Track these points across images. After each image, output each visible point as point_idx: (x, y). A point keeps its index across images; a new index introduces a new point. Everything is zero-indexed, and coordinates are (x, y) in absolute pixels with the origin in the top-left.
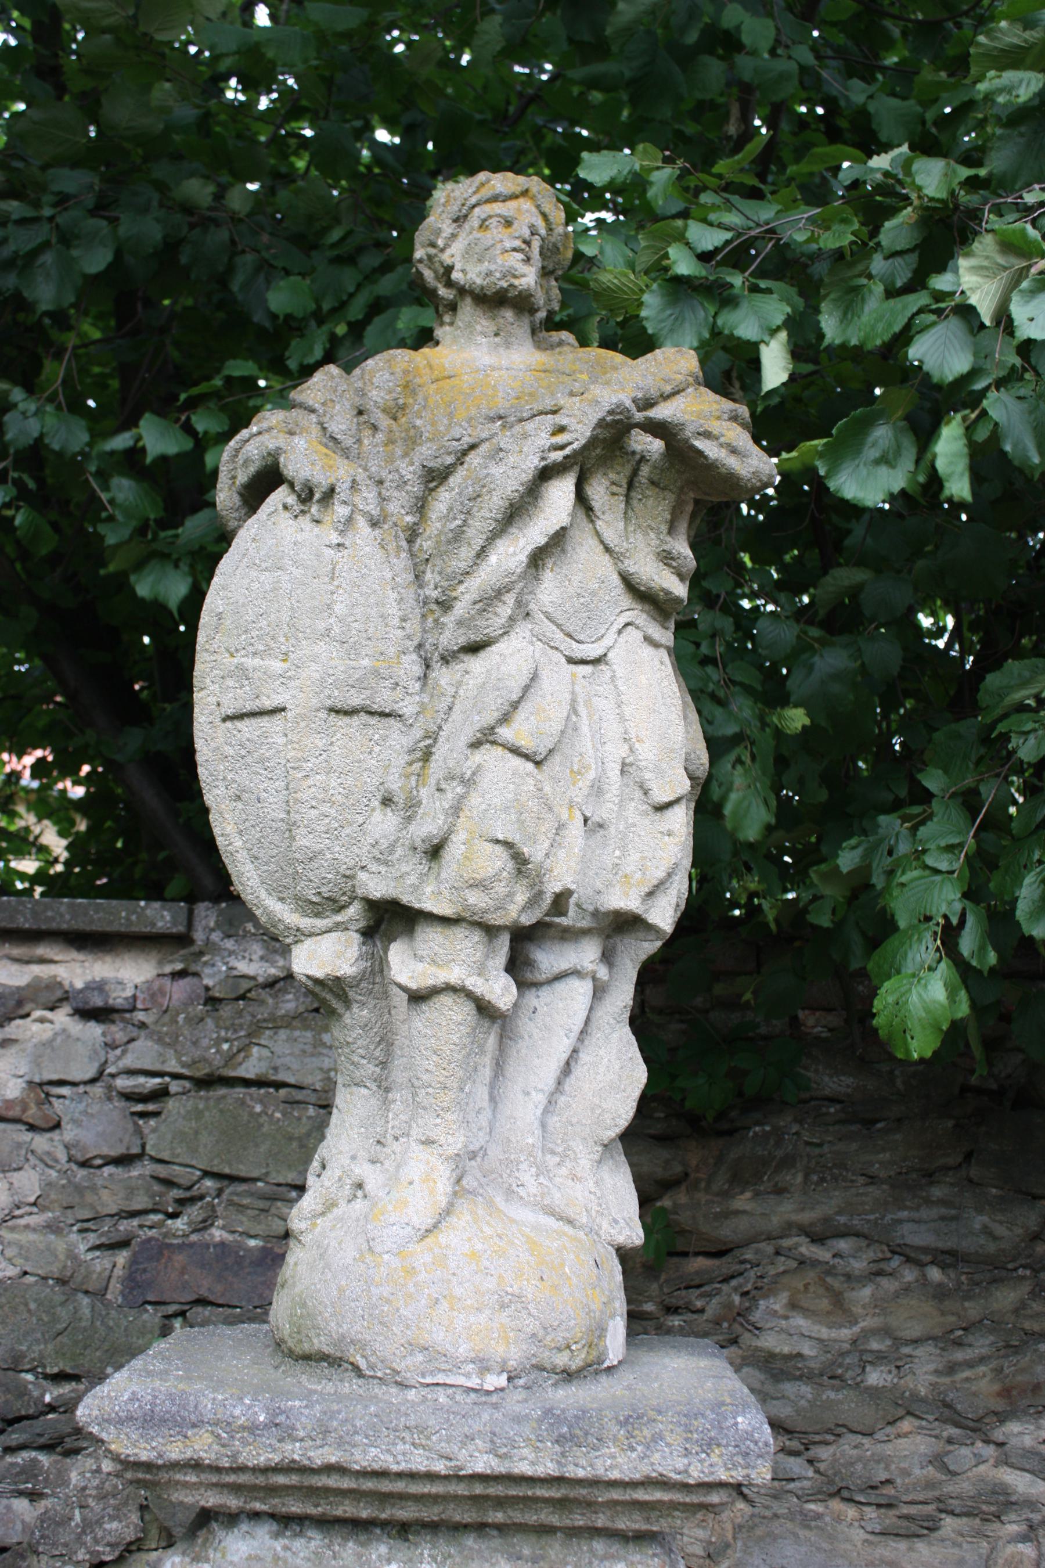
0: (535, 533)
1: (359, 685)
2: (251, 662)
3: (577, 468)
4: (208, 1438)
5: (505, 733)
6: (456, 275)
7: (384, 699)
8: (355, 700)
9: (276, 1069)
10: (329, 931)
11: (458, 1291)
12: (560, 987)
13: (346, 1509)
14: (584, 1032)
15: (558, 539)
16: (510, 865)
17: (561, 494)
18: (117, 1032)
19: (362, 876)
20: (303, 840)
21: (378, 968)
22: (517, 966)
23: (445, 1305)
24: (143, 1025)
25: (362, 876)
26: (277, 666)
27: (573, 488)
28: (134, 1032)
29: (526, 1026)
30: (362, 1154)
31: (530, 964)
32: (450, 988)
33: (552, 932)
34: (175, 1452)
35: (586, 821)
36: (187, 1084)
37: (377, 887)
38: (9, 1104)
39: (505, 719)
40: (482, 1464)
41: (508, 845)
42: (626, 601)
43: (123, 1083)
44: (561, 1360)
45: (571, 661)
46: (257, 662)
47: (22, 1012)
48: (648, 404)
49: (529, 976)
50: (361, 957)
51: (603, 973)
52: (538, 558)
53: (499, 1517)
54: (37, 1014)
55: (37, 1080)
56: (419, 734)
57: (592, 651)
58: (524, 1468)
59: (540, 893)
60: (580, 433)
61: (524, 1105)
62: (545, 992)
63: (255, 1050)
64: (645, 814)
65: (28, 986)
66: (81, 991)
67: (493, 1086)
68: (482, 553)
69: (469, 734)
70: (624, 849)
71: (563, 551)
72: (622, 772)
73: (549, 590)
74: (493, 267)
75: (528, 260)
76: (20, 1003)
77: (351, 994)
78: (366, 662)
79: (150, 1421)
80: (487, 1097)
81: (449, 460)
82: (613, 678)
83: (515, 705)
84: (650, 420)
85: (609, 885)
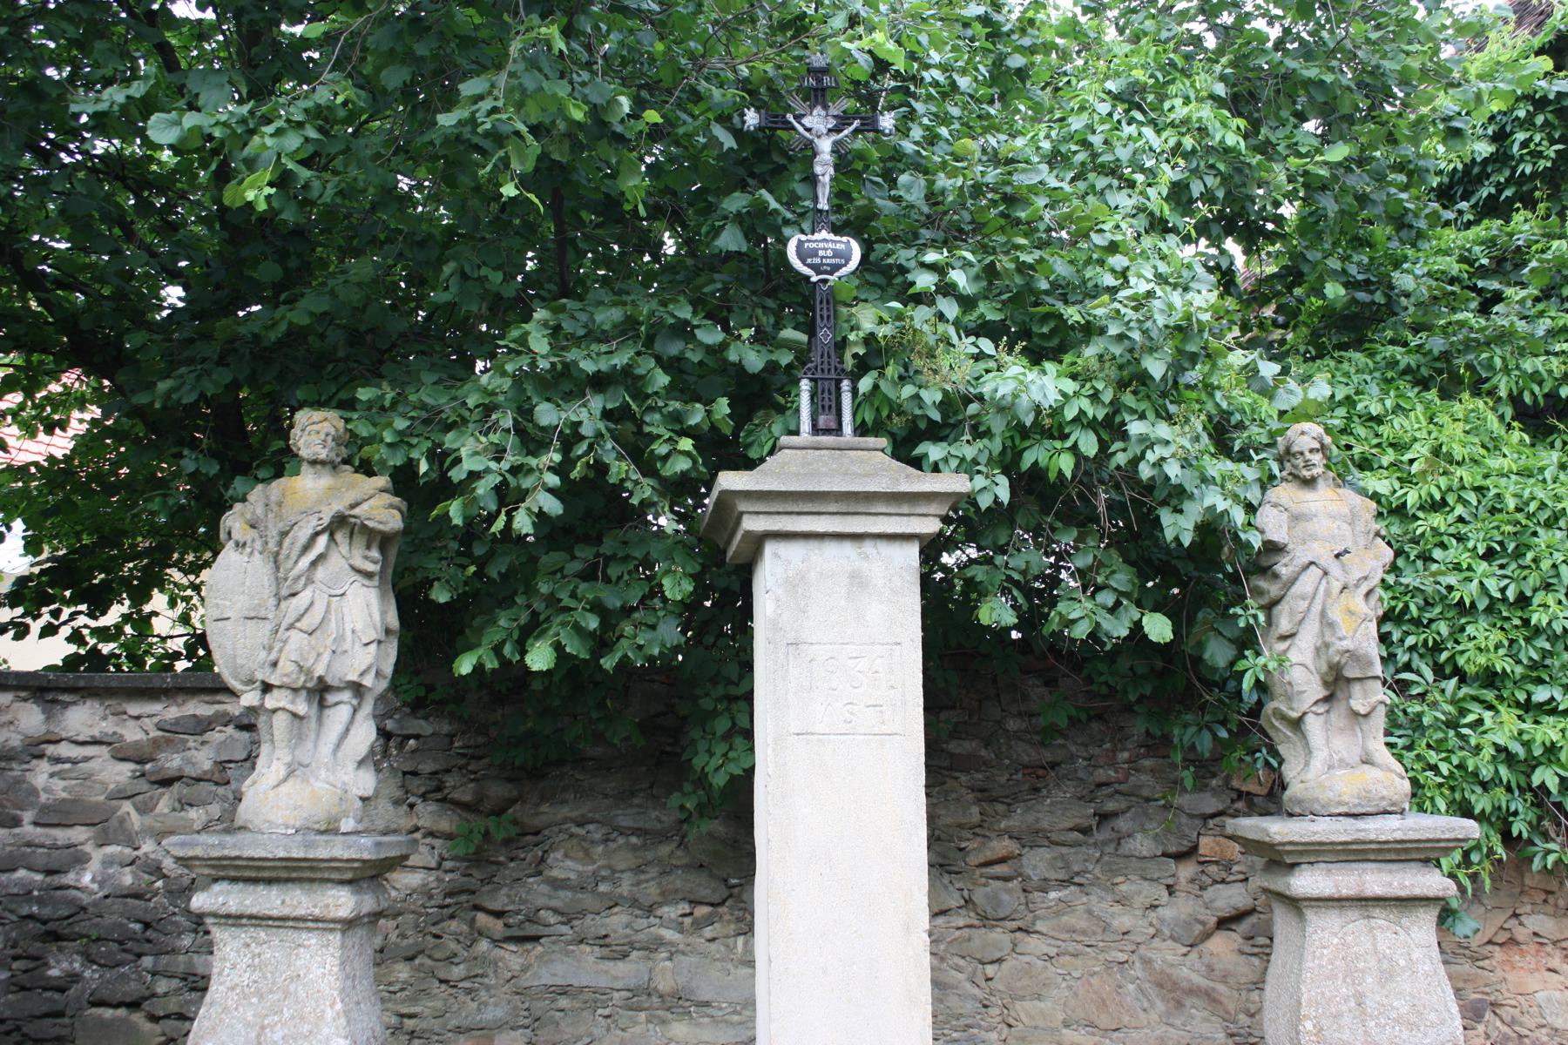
7: (262, 613)
13: (247, 874)
15: (321, 557)
20: (239, 661)
32: (283, 709)
34: (191, 854)
38: (205, 772)
39: (298, 620)
40: (282, 854)
52: (314, 564)
53: (294, 875)
58: (295, 855)
60: (326, 521)
73: (320, 573)
79: (183, 845)
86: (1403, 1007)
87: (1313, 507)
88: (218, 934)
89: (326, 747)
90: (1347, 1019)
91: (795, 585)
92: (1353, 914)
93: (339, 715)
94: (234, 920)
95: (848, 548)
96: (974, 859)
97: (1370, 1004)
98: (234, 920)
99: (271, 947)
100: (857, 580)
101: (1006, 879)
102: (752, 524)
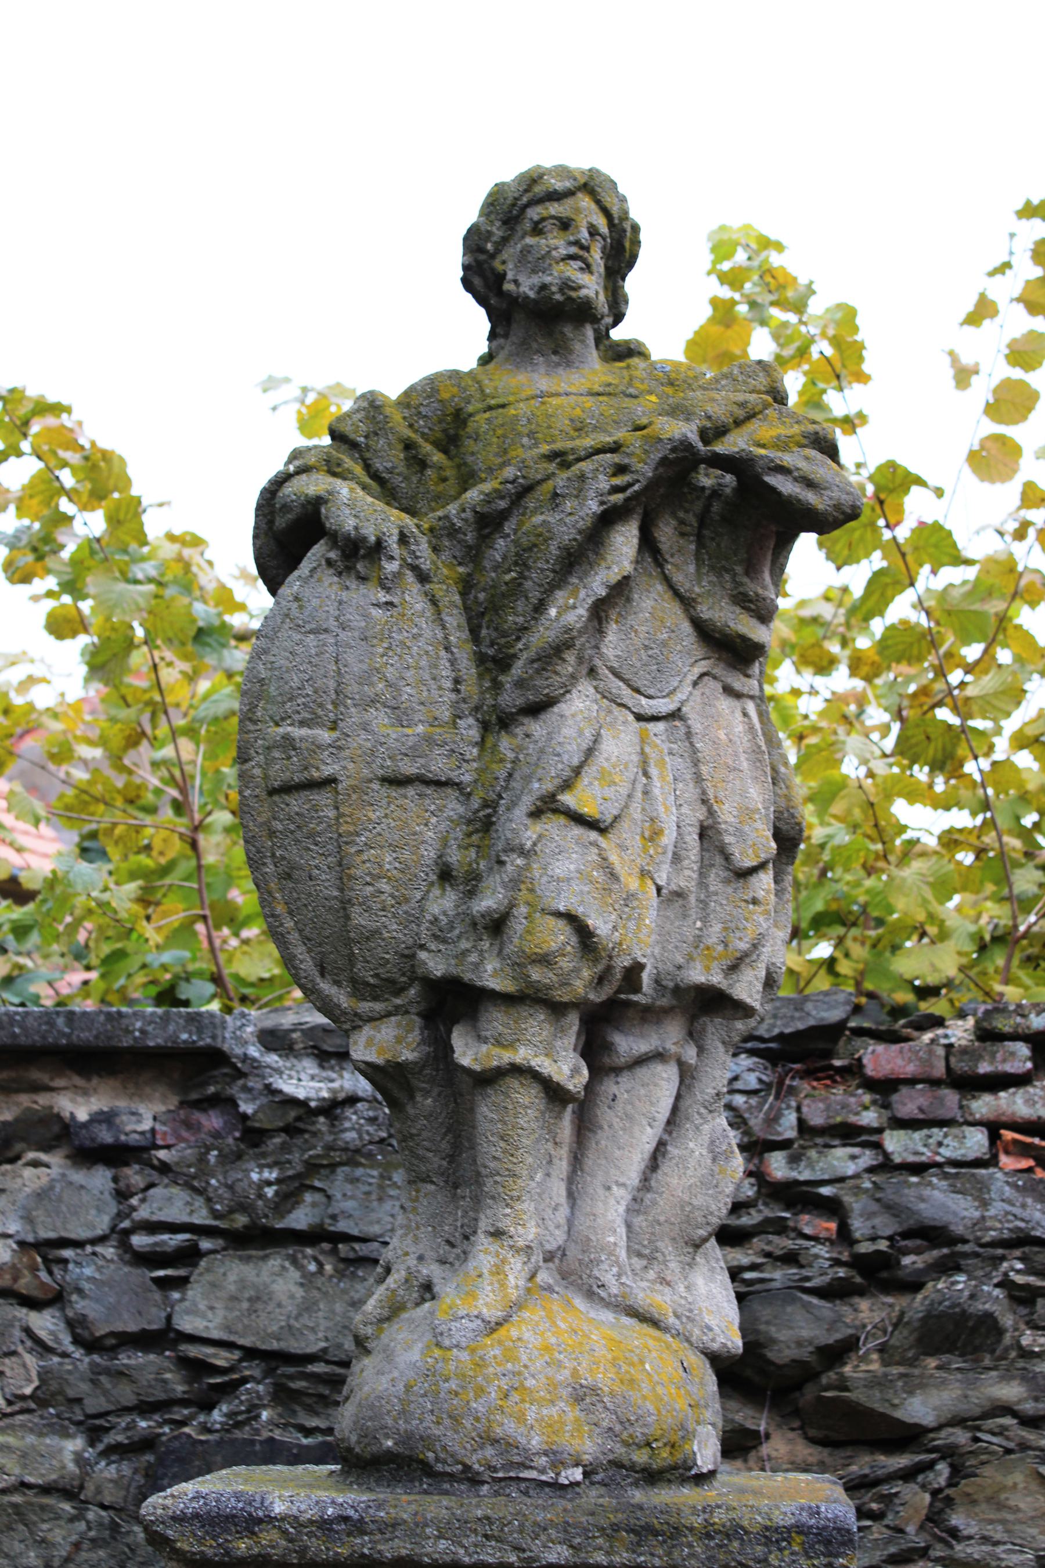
0: (598, 583)
1: (413, 753)
2: (298, 732)
3: (640, 510)
4: (275, 1535)
5: (567, 799)
6: (508, 287)
7: (439, 765)
8: (408, 768)
9: (334, 1217)
10: (389, 1014)
11: (530, 1383)
12: (642, 1072)
14: (672, 1122)
15: (621, 589)
16: (574, 940)
17: (624, 544)
18: (134, 1176)
19: (423, 955)
20: (359, 918)
21: (441, 1051)
22: (594, 1051)
23: (515, 1397)
24: (164, 1168)
25: (423, 955)
26: (325, 736)
27: (635, 532)
28: (155, 1176)
29: (606, 1116)
30: (430, 1254)
31: (608, 1047)
33: (631, 1013)
35: (659, 889)
36: (220, 1243)
37: (436, 965)
39: (567, 785)
41: (571, 918)
42: (699, 652)
43: (139, 1241)
44: (640, 1457)
45: (640, 718)
46: (304, 732)
47: (10, 1154)
48: (721, 432)
49: (607, 1060)
50: (423, 1042)
51: (690, 1054)
52: (600, 611)
54: (31, 1155)
55: (30, 1238)
56: (476, 803)
57: (663, 706)
59: (609, 969)
61: (610, 1211)
62: (625, 1079)
63: (308, 1197)
64: (727, 881)
65: (17, 1120)
66: (85, 1125)
67: (571, 1180)
68: (540, 608)
69: (527, 803)
70: (704, 919)
71: (629, 600)
72: (701, 836)
73: (613, 644)
74: (548, 279)
75: (588, 268)
76: (7, 1143)
77: (415, 1082)
78: (420, 729)
80: (563, 1192)
81: (503, 504)
82: (689, 735)
83: (577, 771)
84: (716, 455)
85: (690, 958)
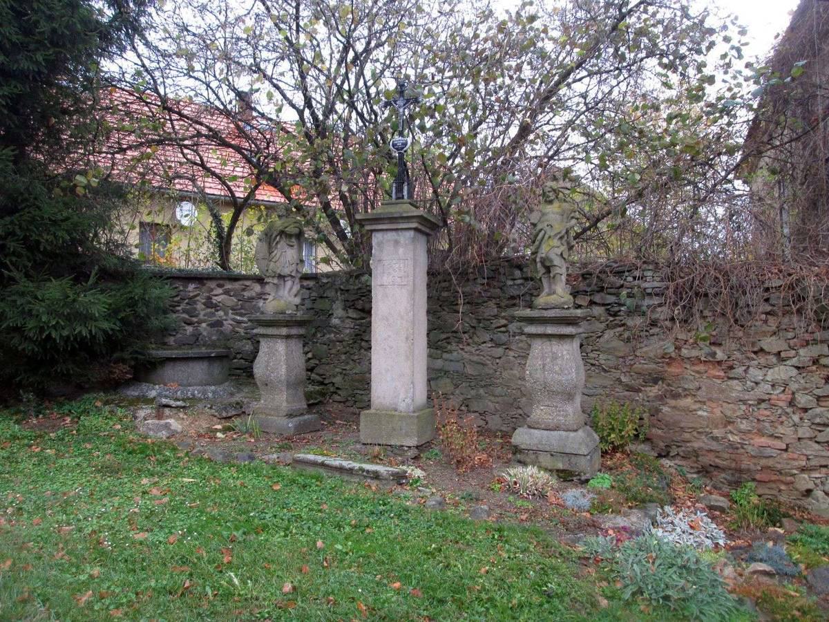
86: (557, 368)
87: (547, 210)
88: (261, 339)
89: (286, 292)
90: (539, 371)
91: (380, 244)
92: (544, 340)
93: (289, 283)
94: (264, 336)
95: (394, 233)
96: (494, 326)
97: (547, 368)
98: (264, 336)
99: (271, 343)
100: (397, 243)
101: (504, 332)
102: (368, 227)
